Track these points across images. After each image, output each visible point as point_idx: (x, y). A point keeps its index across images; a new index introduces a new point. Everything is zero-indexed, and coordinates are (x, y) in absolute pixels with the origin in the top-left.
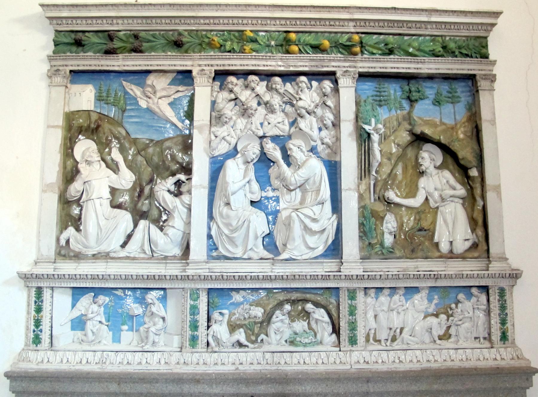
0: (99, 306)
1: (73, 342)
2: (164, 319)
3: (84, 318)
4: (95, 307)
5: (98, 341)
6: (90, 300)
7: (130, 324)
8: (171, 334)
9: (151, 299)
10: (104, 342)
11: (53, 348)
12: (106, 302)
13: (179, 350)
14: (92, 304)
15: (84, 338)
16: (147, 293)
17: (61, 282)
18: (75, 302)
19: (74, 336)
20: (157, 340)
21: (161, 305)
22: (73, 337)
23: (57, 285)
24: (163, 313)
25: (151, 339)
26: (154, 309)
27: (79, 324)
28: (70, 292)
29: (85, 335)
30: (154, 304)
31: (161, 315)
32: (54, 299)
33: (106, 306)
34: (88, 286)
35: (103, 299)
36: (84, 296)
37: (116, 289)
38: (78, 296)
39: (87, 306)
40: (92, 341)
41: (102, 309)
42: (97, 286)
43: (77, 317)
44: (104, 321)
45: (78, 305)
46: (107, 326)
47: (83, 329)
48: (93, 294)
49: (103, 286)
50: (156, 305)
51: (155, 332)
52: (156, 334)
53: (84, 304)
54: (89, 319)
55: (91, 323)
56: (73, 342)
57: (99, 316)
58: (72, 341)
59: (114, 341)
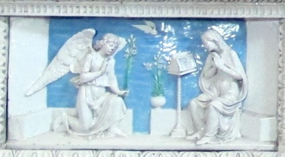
0: (106, 55)
1: (52, 130)
2: (240, 82)
3: (74, 80)
4: (97, 59)
5: (102, 129)
6: (86, 42)
7: (170, 93)
8: (254, 114)
9: (214, 41)
10: (116, 130)
11: (9, 144)
12: (121, 47)
13: (272, 146)
14: (90, 52)
15: (75, 122)
16: (205, 30)
17: (26, 6)
18: (55, 48)
19: (54, 117)
20: (225, 127)
21: (234, 53)
22: (50, 121)
23: (17, 13)
24: (237, 70)
25: (213, 125)
26: (220, 62)
27: (64, 92)
28: (45, 26)
29: (77, 116)
30: (219, 52)
31: (234, 74)
32: (12, 40)
33: (120, 57)
34: (82, 14)
35: (113, 41)
36: (75, 36)
37: (141, 20)
38: (62, 36)
39: (81, 57)
40: (91, 129)
41: (112, 61)
42: (101, 14)
43: (59, 79)
44: (115, 86)
45: (63, 53)
46: (123, 97)
47: (72, 104)
48: (93, 31)
49: (113, 14)
50: (224, 54)
51: (221, 109)
52: (224, 115)
53: (75, 52)
54: (85, 84)
55: (89, 92)
56: (52, 130)
57: (105, 76)
58: (48, 129)
59: (136, 129)
